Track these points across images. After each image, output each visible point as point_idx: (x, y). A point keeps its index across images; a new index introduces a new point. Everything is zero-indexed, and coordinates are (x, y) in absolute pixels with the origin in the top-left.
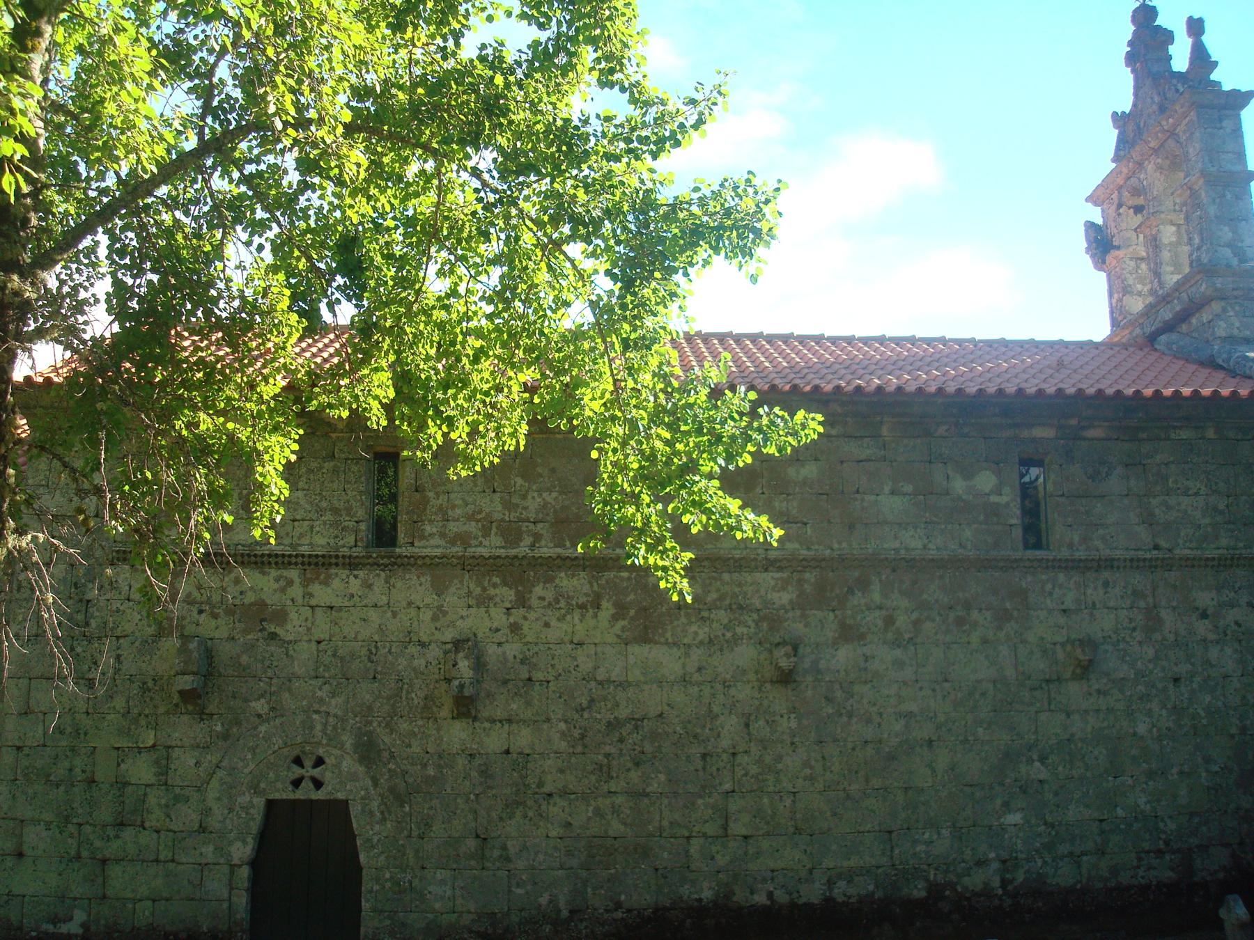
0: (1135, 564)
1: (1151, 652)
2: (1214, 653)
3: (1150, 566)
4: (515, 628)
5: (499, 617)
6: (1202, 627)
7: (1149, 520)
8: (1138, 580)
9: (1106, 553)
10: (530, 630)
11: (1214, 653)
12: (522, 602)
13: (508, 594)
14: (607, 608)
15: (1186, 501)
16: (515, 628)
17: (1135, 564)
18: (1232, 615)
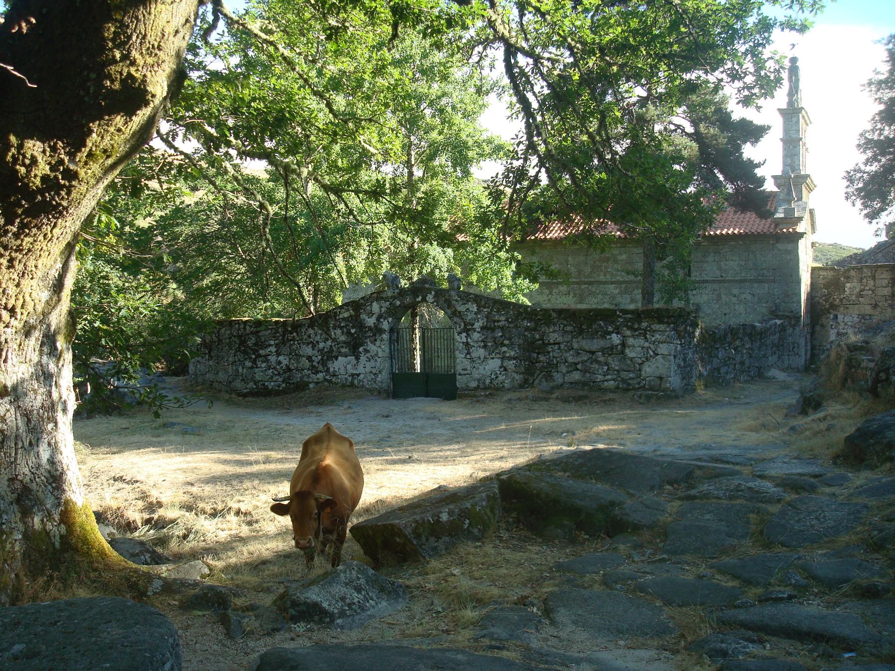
0: (713, 282)
1: (717, 306)
2: (737, 307)
3: (720, 282)
4: (549, 300)
5: (545, 298)
6: (734, 300)
7: (720, 269)
8: (715, 286)
9: (706, 278)
10: (553, 300)
11: (737, 307)
12: (551, 293)
13: (547, 291)
14: (572, 295)
15: (732, 263)
16: (549, 300)
17: (713, 282)
18: (744, 296)
